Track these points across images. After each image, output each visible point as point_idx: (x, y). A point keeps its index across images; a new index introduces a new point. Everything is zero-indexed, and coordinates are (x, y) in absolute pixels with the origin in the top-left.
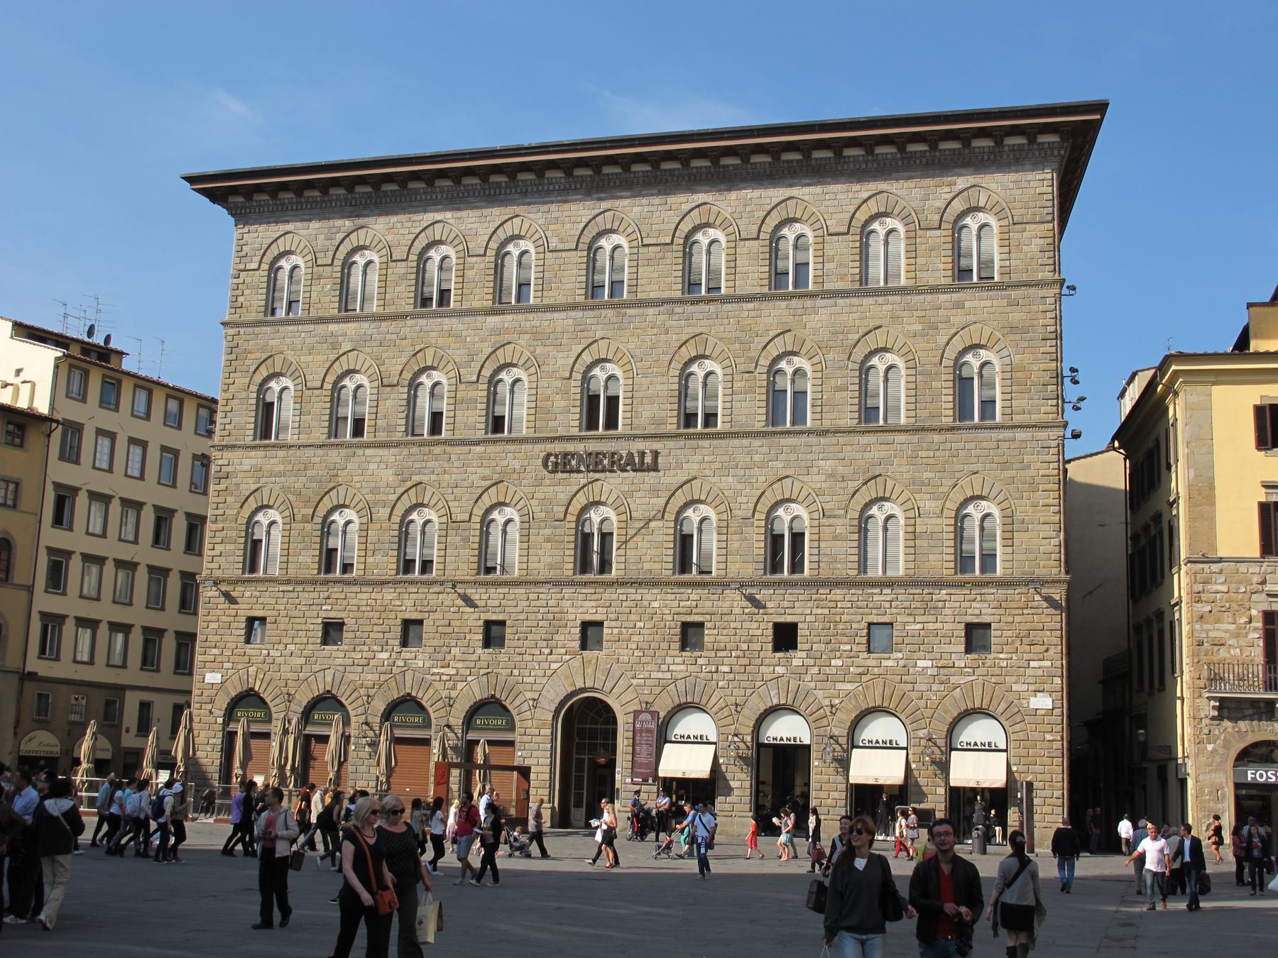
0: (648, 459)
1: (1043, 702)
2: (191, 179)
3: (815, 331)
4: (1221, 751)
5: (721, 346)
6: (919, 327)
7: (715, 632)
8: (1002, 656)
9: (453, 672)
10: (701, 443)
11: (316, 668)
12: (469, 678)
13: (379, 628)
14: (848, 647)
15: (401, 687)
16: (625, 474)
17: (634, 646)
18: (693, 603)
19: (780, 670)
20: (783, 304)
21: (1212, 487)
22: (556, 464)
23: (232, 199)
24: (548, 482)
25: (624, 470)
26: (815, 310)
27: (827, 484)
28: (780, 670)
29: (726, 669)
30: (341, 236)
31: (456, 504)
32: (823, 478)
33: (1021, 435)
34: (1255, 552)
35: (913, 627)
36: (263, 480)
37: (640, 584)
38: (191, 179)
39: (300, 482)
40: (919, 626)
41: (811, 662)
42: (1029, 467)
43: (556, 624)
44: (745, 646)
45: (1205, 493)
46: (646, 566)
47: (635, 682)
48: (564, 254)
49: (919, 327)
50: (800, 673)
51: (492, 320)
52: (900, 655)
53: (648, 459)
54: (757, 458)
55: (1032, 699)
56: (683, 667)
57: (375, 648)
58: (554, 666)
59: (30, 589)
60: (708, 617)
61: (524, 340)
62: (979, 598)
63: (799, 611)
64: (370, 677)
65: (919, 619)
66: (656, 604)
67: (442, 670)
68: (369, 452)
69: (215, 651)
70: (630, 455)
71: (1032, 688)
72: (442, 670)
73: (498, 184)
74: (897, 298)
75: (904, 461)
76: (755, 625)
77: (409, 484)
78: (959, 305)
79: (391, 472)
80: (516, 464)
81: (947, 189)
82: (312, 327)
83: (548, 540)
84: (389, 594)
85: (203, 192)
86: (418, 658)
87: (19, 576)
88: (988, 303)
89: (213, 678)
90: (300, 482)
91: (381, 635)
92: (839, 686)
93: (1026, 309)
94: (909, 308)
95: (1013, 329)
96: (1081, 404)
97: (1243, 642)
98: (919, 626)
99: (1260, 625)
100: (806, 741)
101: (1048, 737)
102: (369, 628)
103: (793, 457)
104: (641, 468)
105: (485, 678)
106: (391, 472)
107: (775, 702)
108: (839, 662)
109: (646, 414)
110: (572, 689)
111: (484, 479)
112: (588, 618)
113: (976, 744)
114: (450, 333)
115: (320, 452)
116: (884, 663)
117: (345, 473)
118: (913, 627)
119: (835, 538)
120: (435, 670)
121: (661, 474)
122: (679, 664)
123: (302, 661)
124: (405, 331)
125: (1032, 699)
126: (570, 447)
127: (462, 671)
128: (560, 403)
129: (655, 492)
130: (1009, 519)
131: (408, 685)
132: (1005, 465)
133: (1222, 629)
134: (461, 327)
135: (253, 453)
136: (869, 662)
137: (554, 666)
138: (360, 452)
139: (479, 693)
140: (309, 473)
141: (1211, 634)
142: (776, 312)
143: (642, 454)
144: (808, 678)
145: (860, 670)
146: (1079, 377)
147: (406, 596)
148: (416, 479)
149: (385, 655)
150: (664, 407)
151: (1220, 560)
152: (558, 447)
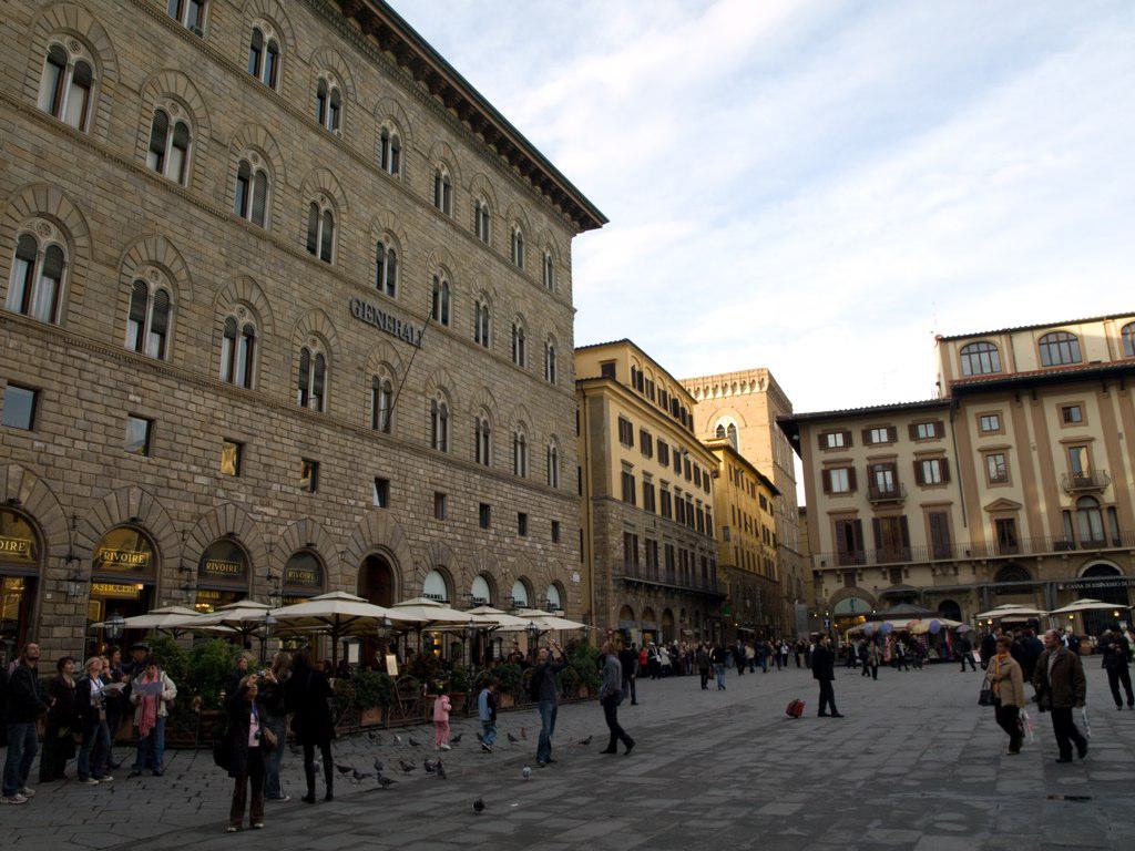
1: (576, 578)
9: (273, 512)
11: (117, 483)
12: (289, 523)
13: (201, 444)
15: (222, 525)
17: (408, 508)
28: (483, 542)
29: (459, 537)
47: (410, 542)
52: (530, 539)
57: (194, 468)
64: (187, 506)
67: (265, 510)
68: (196, 212)
84: (208, 402)
91: (201, 453)
102: (188, 441)
120: (258, 508)
123: (99, 469)
127: (285, 514)
137: (358, 518)
138: (185, 206)
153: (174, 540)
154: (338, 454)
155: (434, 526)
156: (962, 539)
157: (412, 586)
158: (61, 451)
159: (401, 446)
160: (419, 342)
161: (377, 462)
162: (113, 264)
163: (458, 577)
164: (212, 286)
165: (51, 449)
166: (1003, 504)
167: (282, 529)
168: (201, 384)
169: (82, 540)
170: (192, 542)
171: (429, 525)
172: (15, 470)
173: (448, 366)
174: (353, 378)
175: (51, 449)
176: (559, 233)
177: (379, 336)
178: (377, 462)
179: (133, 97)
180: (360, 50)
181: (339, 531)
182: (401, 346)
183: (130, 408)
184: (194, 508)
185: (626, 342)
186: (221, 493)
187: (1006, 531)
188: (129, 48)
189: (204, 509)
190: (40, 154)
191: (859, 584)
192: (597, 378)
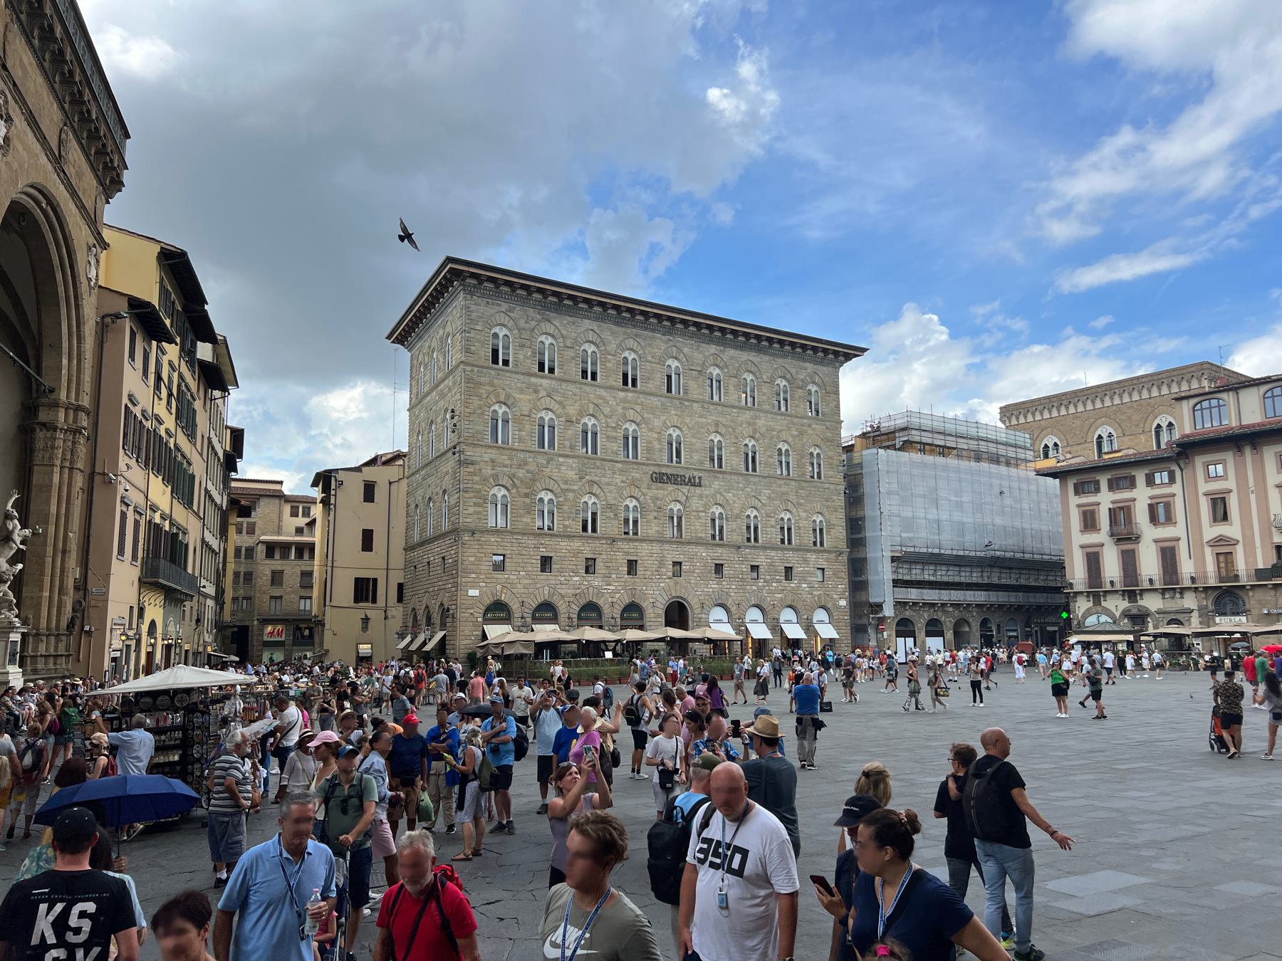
1: (843, 603)
18: (721, 554)
30: (533, 323)
43: (661, 564)
50: (760, 589)
51: (622, 394)
61: (638, 408)
68: (561, 459)
78: (810, 426)
80: (637, 476)
86: (596, 581)
89: (473, 592)
90: (521, 473)
104: (694, 485)
114: (600, 397)
122: (714, 585)
126: (664, 471)
129: (701, 497)
130: (828, 522)
156: (1187, 568)
159: (689, 543)
161: (673, 554)
162: (526, 495)
163: (733, 609)
164: (572, 491)
166: (1220, 541)
172: (499, 587)
176: (824, 370)
177: (671, 487)
178: (673, 554)
180: (646, 329)
182: (685, 489)
187: (1225, 559)
190: (493, 461)
191: (1103, 604)
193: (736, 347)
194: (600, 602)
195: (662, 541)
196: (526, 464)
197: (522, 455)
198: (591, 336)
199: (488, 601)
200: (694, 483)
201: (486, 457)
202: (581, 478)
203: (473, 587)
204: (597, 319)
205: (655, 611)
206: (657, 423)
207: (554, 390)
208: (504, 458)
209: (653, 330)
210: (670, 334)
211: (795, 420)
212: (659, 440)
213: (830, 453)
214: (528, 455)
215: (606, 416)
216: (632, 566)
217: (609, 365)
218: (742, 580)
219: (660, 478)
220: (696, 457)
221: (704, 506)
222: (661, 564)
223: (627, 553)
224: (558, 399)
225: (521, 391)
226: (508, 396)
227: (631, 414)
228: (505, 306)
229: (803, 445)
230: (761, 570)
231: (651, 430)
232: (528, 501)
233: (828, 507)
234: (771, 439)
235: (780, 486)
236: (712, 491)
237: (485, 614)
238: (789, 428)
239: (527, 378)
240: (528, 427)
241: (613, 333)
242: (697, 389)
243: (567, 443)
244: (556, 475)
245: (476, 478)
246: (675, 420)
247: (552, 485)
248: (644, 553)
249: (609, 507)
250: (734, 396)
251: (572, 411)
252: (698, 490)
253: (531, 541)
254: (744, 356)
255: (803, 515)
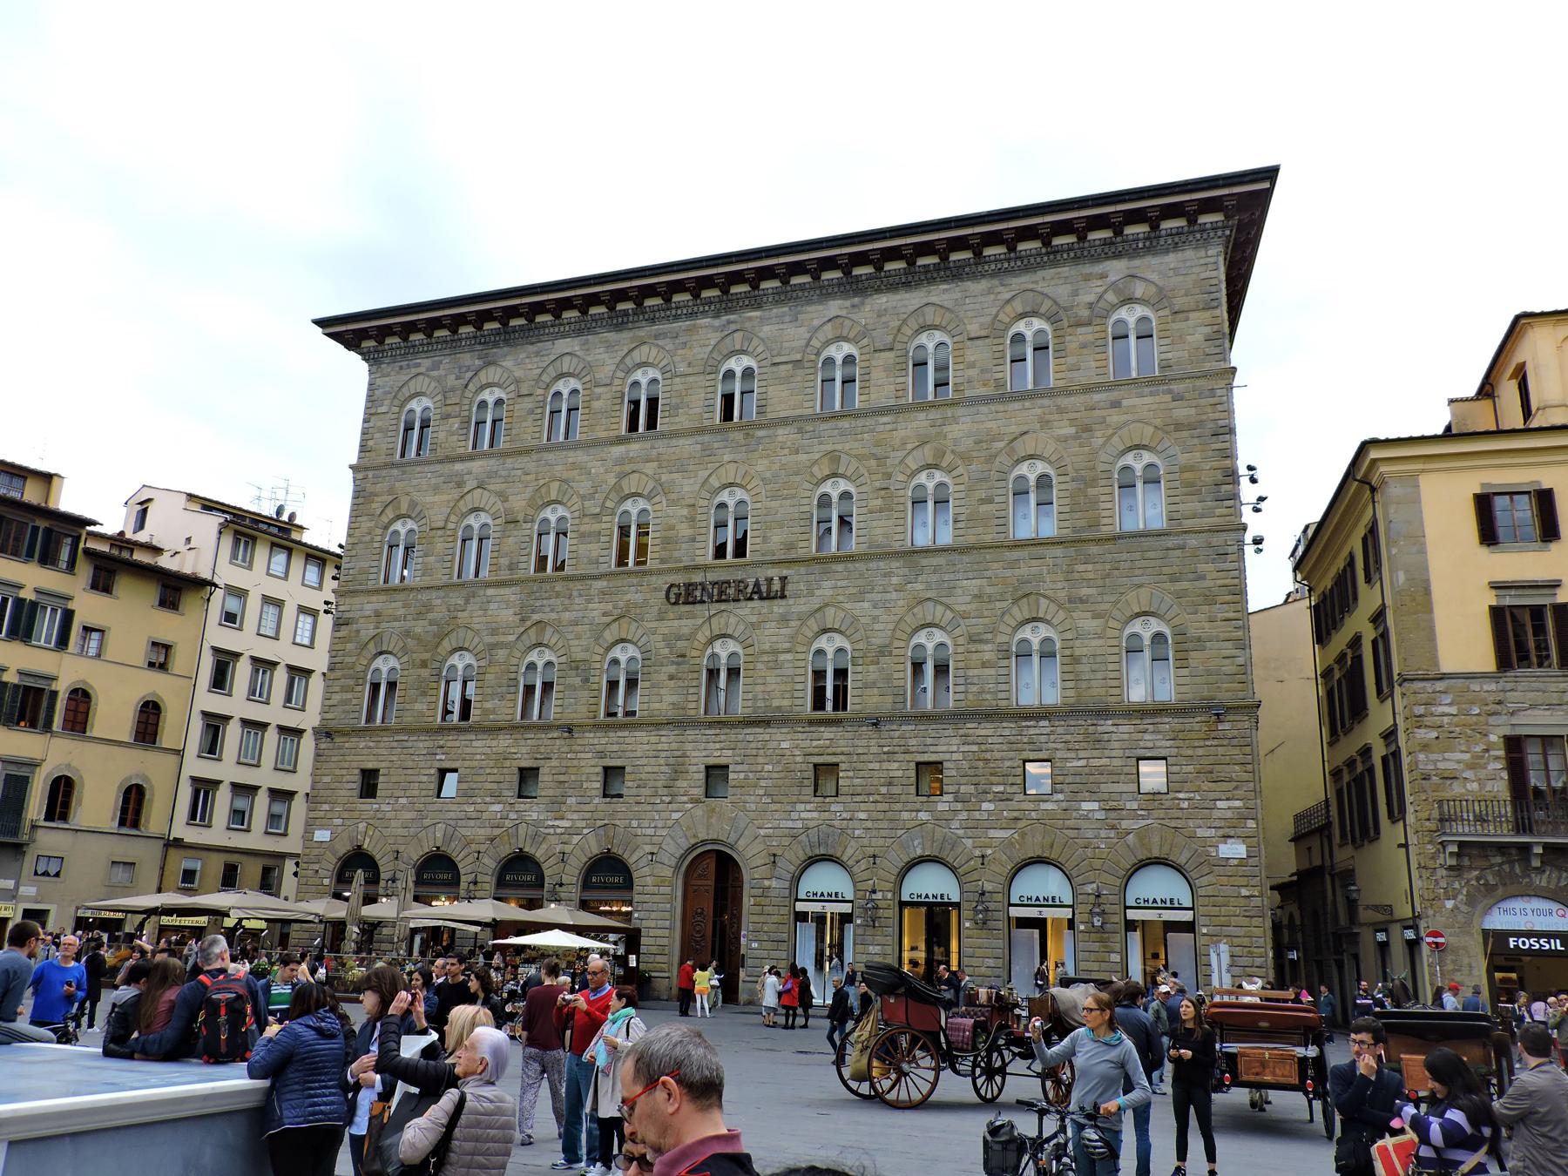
0: (776, 586)
2: (320, 323)
3: (956, 441)
4: (1464, 908)
5: (854, 464)
6: (1072, 430)
7: (851, 774)
8: (1181, 795)
10: (834, 567)
11: (427, 822)
14: (1001, 788)
16: (750, 604)
17: (761, 792)
19: (923, 816)
20: (922, 416)
21: (1427, 591)
22: (678, 595)
23: (365, 344)
24: (671, 616)
25: (751, 599)
26: (955, 420)
27: (974, 606)
28: (923, 816)
29: (863, 816)
30: (470, 374)
31: (576, 642)
32: (968, 599)
33: (1193, 541)
34: (1488, 663)
35: (1076, 763)
36: (384, 625)
37: (765, 723)
38: (320, 323)
39: (419, 627)
40: (1082, 763)
41: (959, 806)
42: (1203, 578)
43: (678, 771)
44: (884, 790)
45: (1421, 596)
46: (776, 703)
47: (762, 832)
48: (691, 379)
49: (1072, 430)
50: (942, 820)
51: (617, 450)
53: (776, 586)
54: (895, 580)
55: (1222, 847)
56: (815, 815)
58: (676, 816)
59: (179, 753)
60: (842, 758)
61: (650, 468)
62: (1151, 728)
63: (944, 748)
64: (482, 831)
65: (1082, 754)
66: (784, 745)
67: (557, 823)
68: (490, 592)
69: (326, 807)
70: (757, 584)
71: (1221, 832)
72: (557, 823)
73: (625, 313)
74: (1046, 402)
75: (1060, 577)
76: (896, 765)
77: (529, 623)
78: (1116, 404)
79: (511, 611)
80: (639, 598)
81: (1099, 283)
82: (438, 467)
83: (671, 678)
84: (503, 742)
85: (334, 336)
86: (533, 811)
87: (167, 738)
88: (1149, 400)
91: (495, 786)
92: (992, 833)
93: (1194, 403)
94: (1061, 410)
95: (1179, 427)
96: (1262, 505)
97: (1482, 774)
98: (1082, 763)
99: (1502, 753)
100: (955, 898)
101: (1244, 892)
103: (934, 578)
105: (601, 832)
106: (511, 611)
107: (919, 852)
108: (991, 806)
109: (776, 539)
110: (693, 841)
111: (605, 614)
112: (711, 761)
113: (1155, 901)
115: (441, 593)
116: (1044, 806)
117: (465, 614)
118: (1076, 763)
119: (984, 665)
121: (791, 601)
122: (807, 813)
124: (531, 466)
125: (1222, 847)
126: (697, 578)
128: (685, 531)
129: (784, 619)
130: (1180, 633)
131: (521, 839)
132: (1174, 578)
133: (1453, 760)
134: (586, 458)
135: (374, 599)
136: (1025, 806)
137: (676, 816)
139: (595, 849)
140: (430, 616)
141: (1441, 765)
142: (914, 424)
143: (770, 580)
144: (955, 824)
145: (1016, 814)
146: (1258, 475)
147: (522, 742)
148: (536, 617)
149: (497, 807)
150: (795, 530)
151: (1443, 677)
152: (680, 579)
153: (470, 859)
154: (651, 754)
155: (809, 807)
157: (767, 883)
158: (389, 808)
160: (783, 589)
161: (704, 750)
162: (424, 664)
165: (384, 807)
167: (576, 839)
168: (494, 730)
169: (402, 866)
170: (486, 860)
171: (800, 807)
172: (362, 826)
173: (841, 598)
174: (672, 669)
175: (384, 807)
178: (704, 750)
179: (440, 533)
180: (677, 318)
181: (650, 832)
183: (438, 765)
184: (488, 832)
185: (1517, 319)
186: (513, 816)
188: (436, 498)
189: (497, 832)
192: (1435, 437)
193: (892, 287)
194: (539, 854)
195: (680, 724)
196: (428, 607)
197: (424, 597)
198: (567, 365)
199: (343, 848)
200: (762, 593)
201: (369, 609)
202: (523, 620)
203: (322, 827)
204: (579, 332)
205: (478, 864)
206: (688, 486)
207: (492, 475)
208: (396, 606)
209: (692, 315)
210: (728, 310)
211: (1064, 402)
212: (692, 519)
213: (1183, 459)
214: (434, 594)
215: (583, 498)
216: (612, 774)
217: (596, 405)
218: (890, 798)
219: (685, 596)
220: (777, 538)
221: (792, 638)
222: (678, 771)
223: (602, 754)
224: (497, 487)
225: (436, 489)
226: (413, 504)
227: (631, 485)
228: (426, 363)
229: (1095, 453)
230: (950, 771)
231: (672, 503)
232: (425, 673)
233: (1179, 595)
234: (991, 458)
235: (1013, 564)
236: (815, 603)
237: (419, 874)
238: (1045, 423)
239: (446, 468)
240: (440, 546)
241: (609, 347)
242: (782, 399)
243: (504, 561)
244: (478, 621)
245: (350, 646)
246: (729, 473)
247: (469, 639)
248: (641, 751)
249: (574, 665)
250: (882, 387)
251: (518, 503)
252: (778, 607)
253: (422, 744)
254: (910, 300)
255: (1089, 624)
